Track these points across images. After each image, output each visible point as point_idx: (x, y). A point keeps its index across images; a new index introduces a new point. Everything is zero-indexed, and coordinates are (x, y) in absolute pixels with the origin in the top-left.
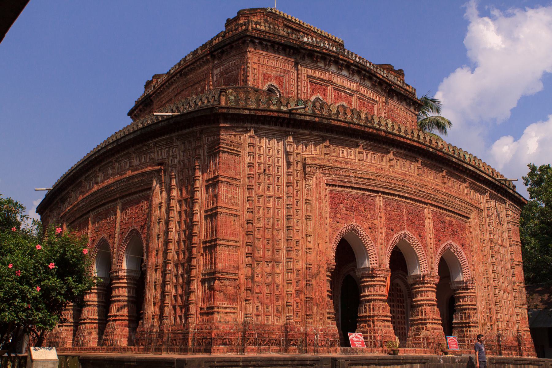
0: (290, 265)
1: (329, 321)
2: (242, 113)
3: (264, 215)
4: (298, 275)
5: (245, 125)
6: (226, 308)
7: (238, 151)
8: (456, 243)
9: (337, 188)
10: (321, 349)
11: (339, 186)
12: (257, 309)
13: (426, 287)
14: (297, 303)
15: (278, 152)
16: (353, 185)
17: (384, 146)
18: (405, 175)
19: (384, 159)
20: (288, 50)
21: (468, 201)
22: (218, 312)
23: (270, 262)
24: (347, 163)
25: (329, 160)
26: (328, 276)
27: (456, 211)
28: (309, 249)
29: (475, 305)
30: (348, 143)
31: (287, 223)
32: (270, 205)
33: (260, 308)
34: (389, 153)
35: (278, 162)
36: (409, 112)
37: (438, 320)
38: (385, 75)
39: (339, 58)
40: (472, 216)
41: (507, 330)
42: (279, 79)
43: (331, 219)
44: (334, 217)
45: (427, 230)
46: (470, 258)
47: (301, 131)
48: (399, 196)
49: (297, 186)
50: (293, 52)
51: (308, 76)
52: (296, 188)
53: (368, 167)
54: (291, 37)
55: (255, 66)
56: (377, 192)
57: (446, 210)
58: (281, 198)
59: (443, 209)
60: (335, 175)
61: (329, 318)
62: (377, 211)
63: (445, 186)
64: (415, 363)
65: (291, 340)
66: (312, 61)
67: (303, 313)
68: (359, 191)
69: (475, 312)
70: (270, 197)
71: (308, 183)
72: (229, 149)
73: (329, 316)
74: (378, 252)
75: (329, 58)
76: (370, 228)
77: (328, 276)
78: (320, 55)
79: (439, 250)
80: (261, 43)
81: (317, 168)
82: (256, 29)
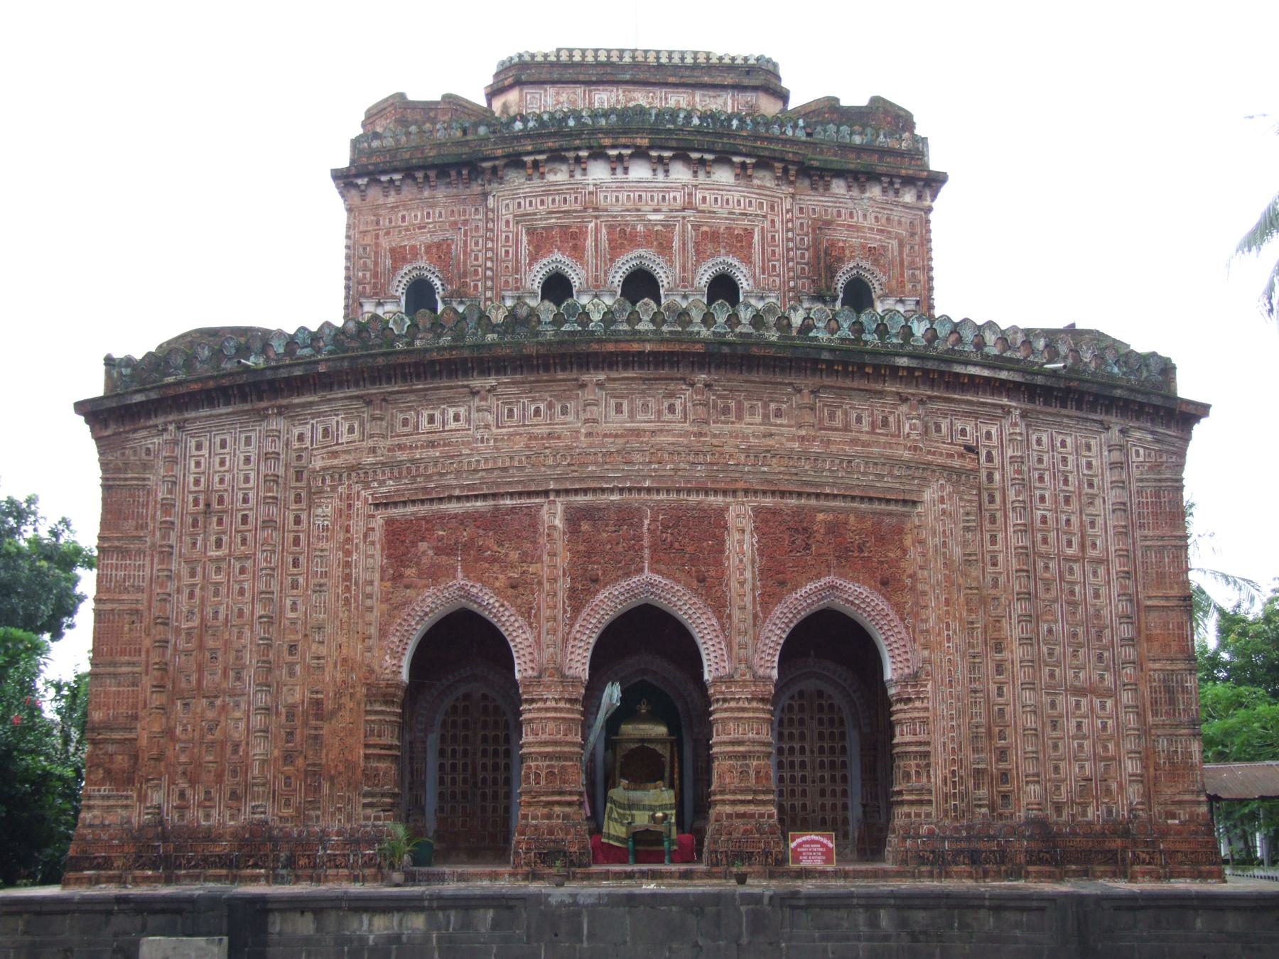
0: (262, 699)
1: (369, 811)
2: (128, 402)
3: (203, 599)
4: (291, 716)
5: (151, 423)
6: (108, 797)
7: (144, 479)
8: (855, 579)
9: (410, 509)
10: (330, 872)
11: (414, 502)
12: (182, 795)
13: (726, 710)
14: (288, 778)
15: (247, 460)
16: (457, 492)
18: (637, 433)
19: (571, 406)
20: (453, 173)
21: (907, 455)
22: (90, 808)
23: (216, 697)
24: (432, 444)
25: (373, 450)
26: (376, 713)
27: (856, 493)
28: (318, 658)
29: (928, 743)
30: (443, 393)
31: (259, 611)
32: (219, 578)
33: (189, 793)
34: (583, 386)
35: (247, 480)
36: (897, 214)
37: (755, 792)
38: (801, 134)
39: (605, 147)
40: (927, 496)
41: (1085, 806)
42: (440, 252)
43: (389, 584)
44: (397, 577)
45: (732, 561)
46: (917, 615)
47: (296, 401)
48: (621, 490)
49: (298, 521)
50: (469, 173)
51: (519, 219)
52: (296, 528)
53: (496, 440)
54: (469, 137)
55: (368, 240)
56: (546, 493)
57: (817, 496)
58: (247, 557)
59: (800, 494)
61: (365, 806)
62: (542, 540)
63: (804, 433)
64: (477, 907)
65: (251, 856)
66: (530, 178)
67: (297, 799)
68: (479, 504)
70: (219, 559)
71: (319, 511)
72: (120, 479)
73: (369, 800)
74: (538, 641)
75: (571, 154)
76: (514, 587)
77: (376, 713)
79: (778, 610)
80: (374, 181)
81: (341, 476)
82: (372, 152)
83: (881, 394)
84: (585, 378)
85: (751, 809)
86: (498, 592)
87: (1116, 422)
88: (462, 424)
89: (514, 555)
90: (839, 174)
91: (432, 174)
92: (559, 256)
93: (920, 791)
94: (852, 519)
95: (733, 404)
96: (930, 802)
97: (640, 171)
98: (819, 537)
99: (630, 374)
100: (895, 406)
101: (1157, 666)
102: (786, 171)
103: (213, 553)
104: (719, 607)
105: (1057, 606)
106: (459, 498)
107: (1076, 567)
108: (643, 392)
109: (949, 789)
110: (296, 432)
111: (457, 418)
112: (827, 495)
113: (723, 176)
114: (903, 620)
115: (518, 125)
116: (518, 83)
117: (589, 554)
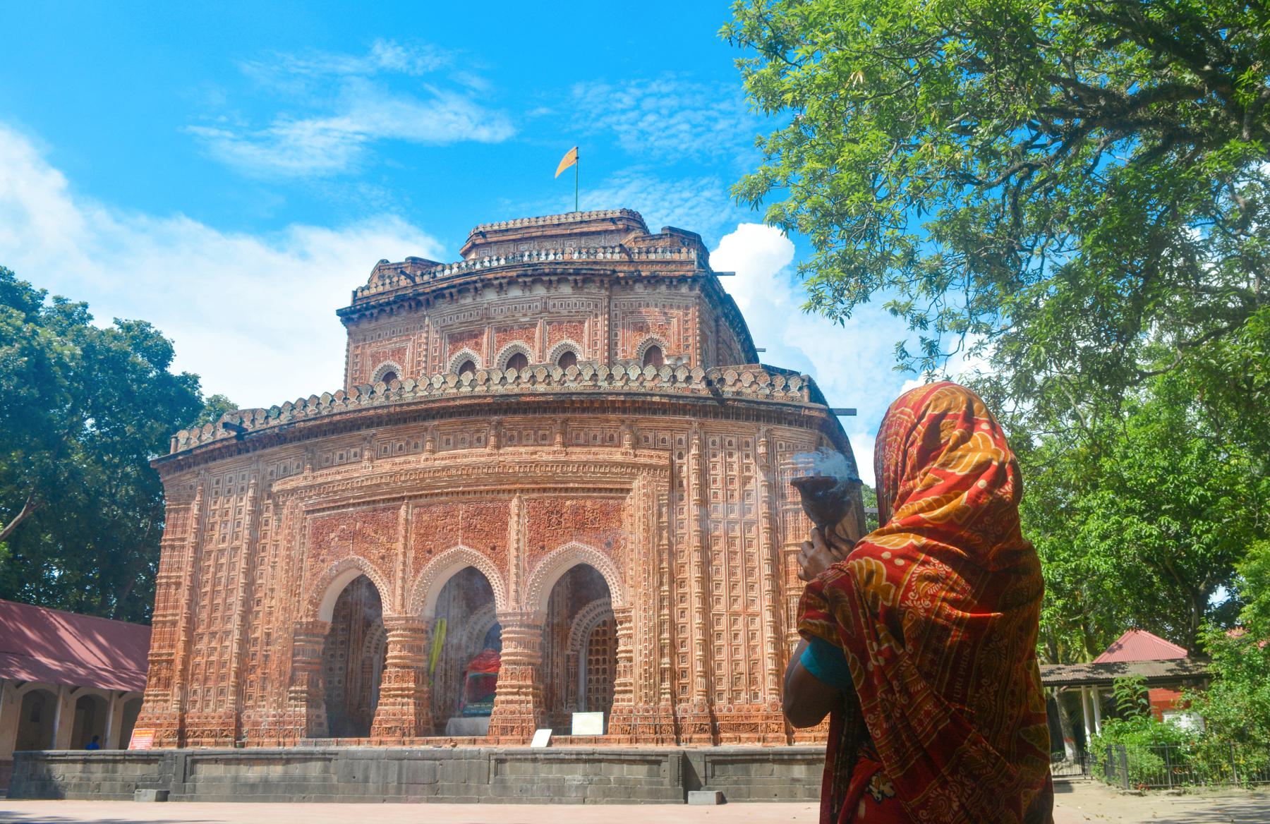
11: (328, 509)
17: (413, 424)
22: (148, 701)
29: (631, 651)
32: (223, 561)
34: (426, 430)
37: (520, 687)
40: (635, 484)
44: (316, 556)
45: (513, 535)
57: (566, 490)
60: (319, 495)
61: (290, 699)
64: (311, 760)
69: (628, 664)
75: (471, 287)
78: (453, 290)
80: (362, 316)
83: (608, 421)
84: (426, 424)
85: (517, 697)
86: (372, 562)
87: (764, 428)
88: (358, 458)
89: (383, 539)
90: (639, 279)
91: (395, 307)
92: (466, 350)
93: (625, 685)
94: (589, 503)
95: (515, 433)
96: (631, 691)
97: (515, 292)
98: (566, 516)
99: (453, 420)
100: (617, 427)
101: (793, 592)
102: (602, 281)
103: (221, 546)
104: (502, 566)
105: (722, 554)
106: (354, 505)
107: (737, 527)
108: (462, 431)
109: (642, 682)
110: (269, 470)
111: (355, 455)
112: (572, 489)
113: (566, 290)
114: (618, 568)
115: (447, 272)
116: (474, 246)
117: (426, 535)
